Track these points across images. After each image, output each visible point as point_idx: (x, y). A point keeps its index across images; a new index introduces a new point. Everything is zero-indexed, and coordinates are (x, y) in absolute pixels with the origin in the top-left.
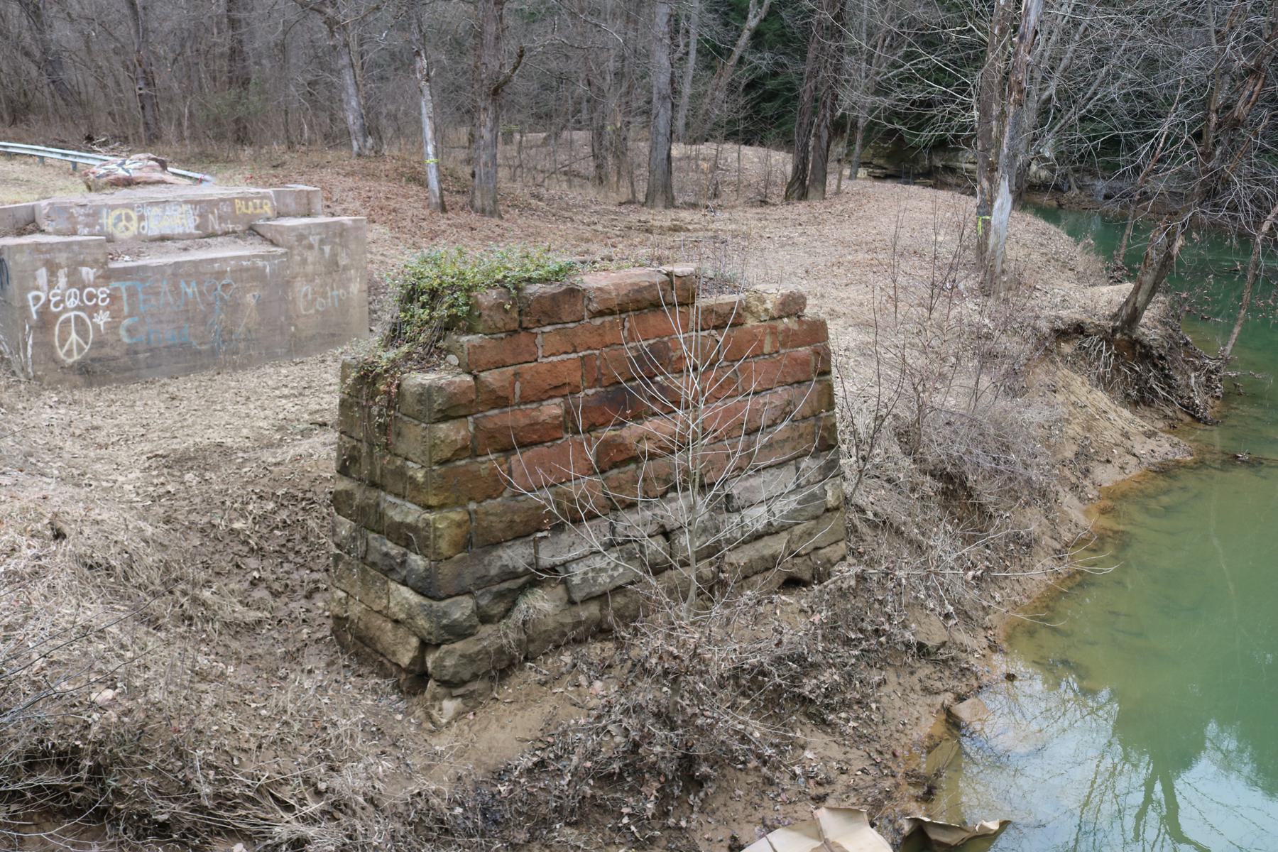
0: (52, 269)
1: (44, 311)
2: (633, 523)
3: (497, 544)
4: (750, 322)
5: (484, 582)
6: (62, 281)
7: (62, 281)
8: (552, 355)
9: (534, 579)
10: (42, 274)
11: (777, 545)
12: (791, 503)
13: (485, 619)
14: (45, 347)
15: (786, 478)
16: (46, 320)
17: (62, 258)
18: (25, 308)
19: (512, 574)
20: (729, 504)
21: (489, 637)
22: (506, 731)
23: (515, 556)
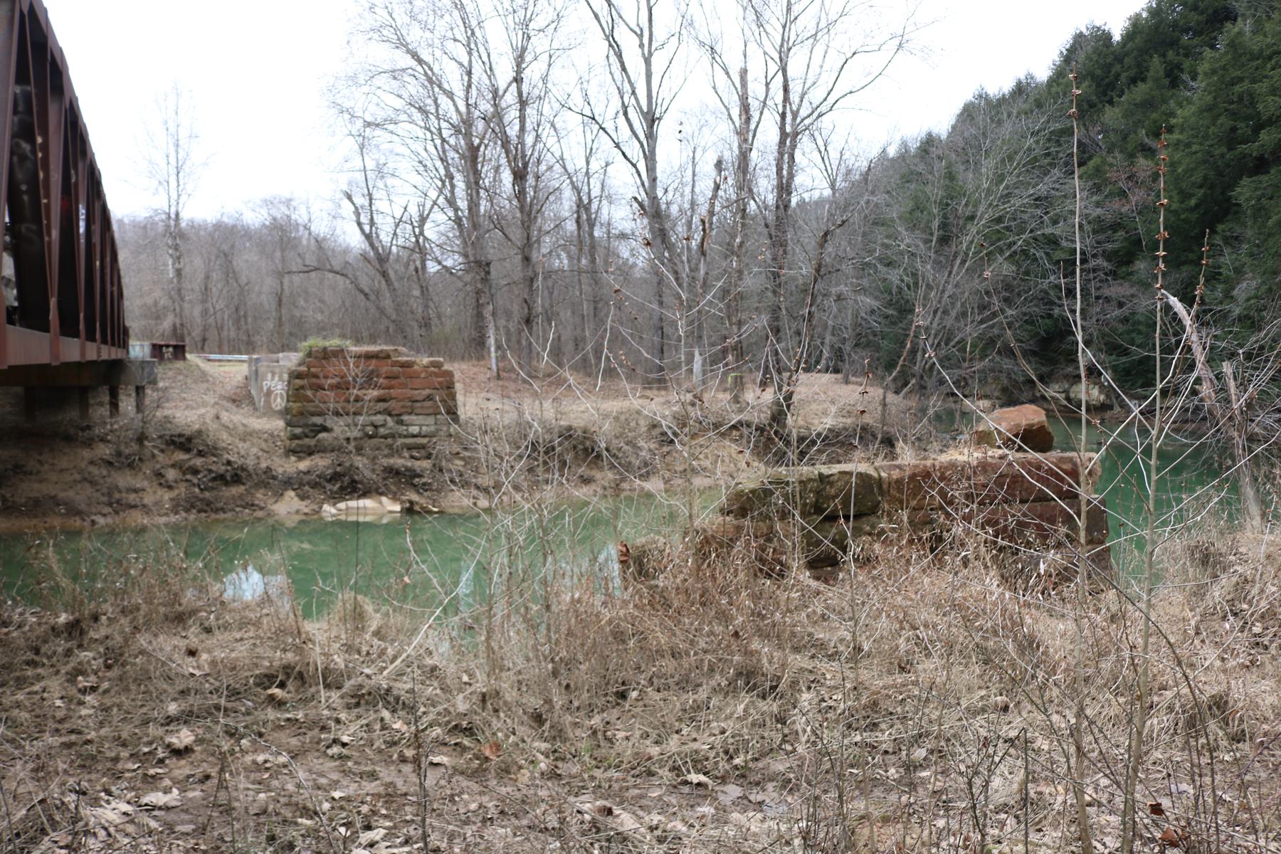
0: (273, 374)
1: (269, 389)
2: (361, 419)
3: (313, 414)
4: (416, 367)
5: (306, 425)
6: (277, 378)
7: (277, 378)
8: (334, 367)
9: (325, 429)
10: (269, 376)
11: (424, 441)
12: (432, 428)
13: (307, 436)
14: (268, 403)
15: (431, 420)
16: (269, 393)
17: (277, 370)
18: (262, 388)
19: (315, 425)
20: (401, 423)
21: (307, 441)
22: (304, 465)
23: (318, 420)
